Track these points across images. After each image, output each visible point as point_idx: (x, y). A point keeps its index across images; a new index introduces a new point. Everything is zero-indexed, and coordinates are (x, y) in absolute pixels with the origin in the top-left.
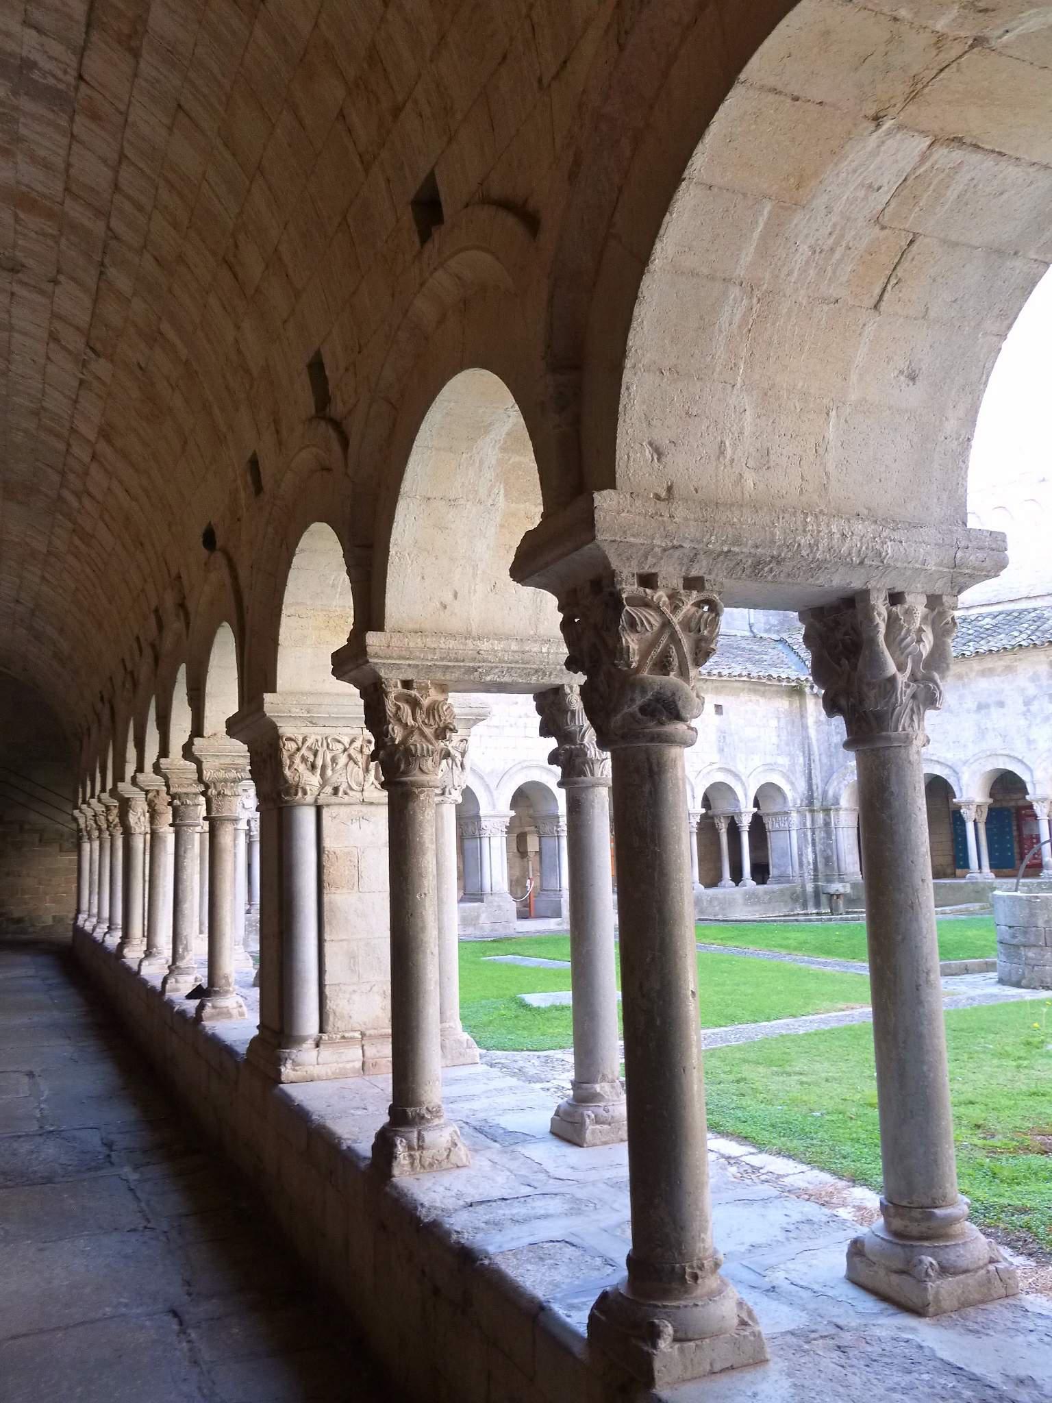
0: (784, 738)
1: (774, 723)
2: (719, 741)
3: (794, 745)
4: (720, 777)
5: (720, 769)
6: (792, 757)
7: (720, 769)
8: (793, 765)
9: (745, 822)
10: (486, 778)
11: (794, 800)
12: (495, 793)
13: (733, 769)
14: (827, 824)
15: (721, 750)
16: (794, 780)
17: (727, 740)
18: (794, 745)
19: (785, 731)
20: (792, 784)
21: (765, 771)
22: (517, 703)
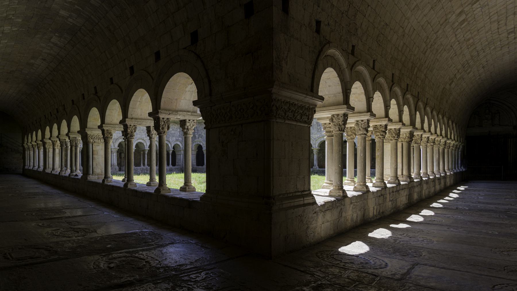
0: (181, 133)
6: (182, 138)
8: (182, 140)
9: (171, 152)
11: (182, 148)
13: (169, 140)
21: (176, 141)
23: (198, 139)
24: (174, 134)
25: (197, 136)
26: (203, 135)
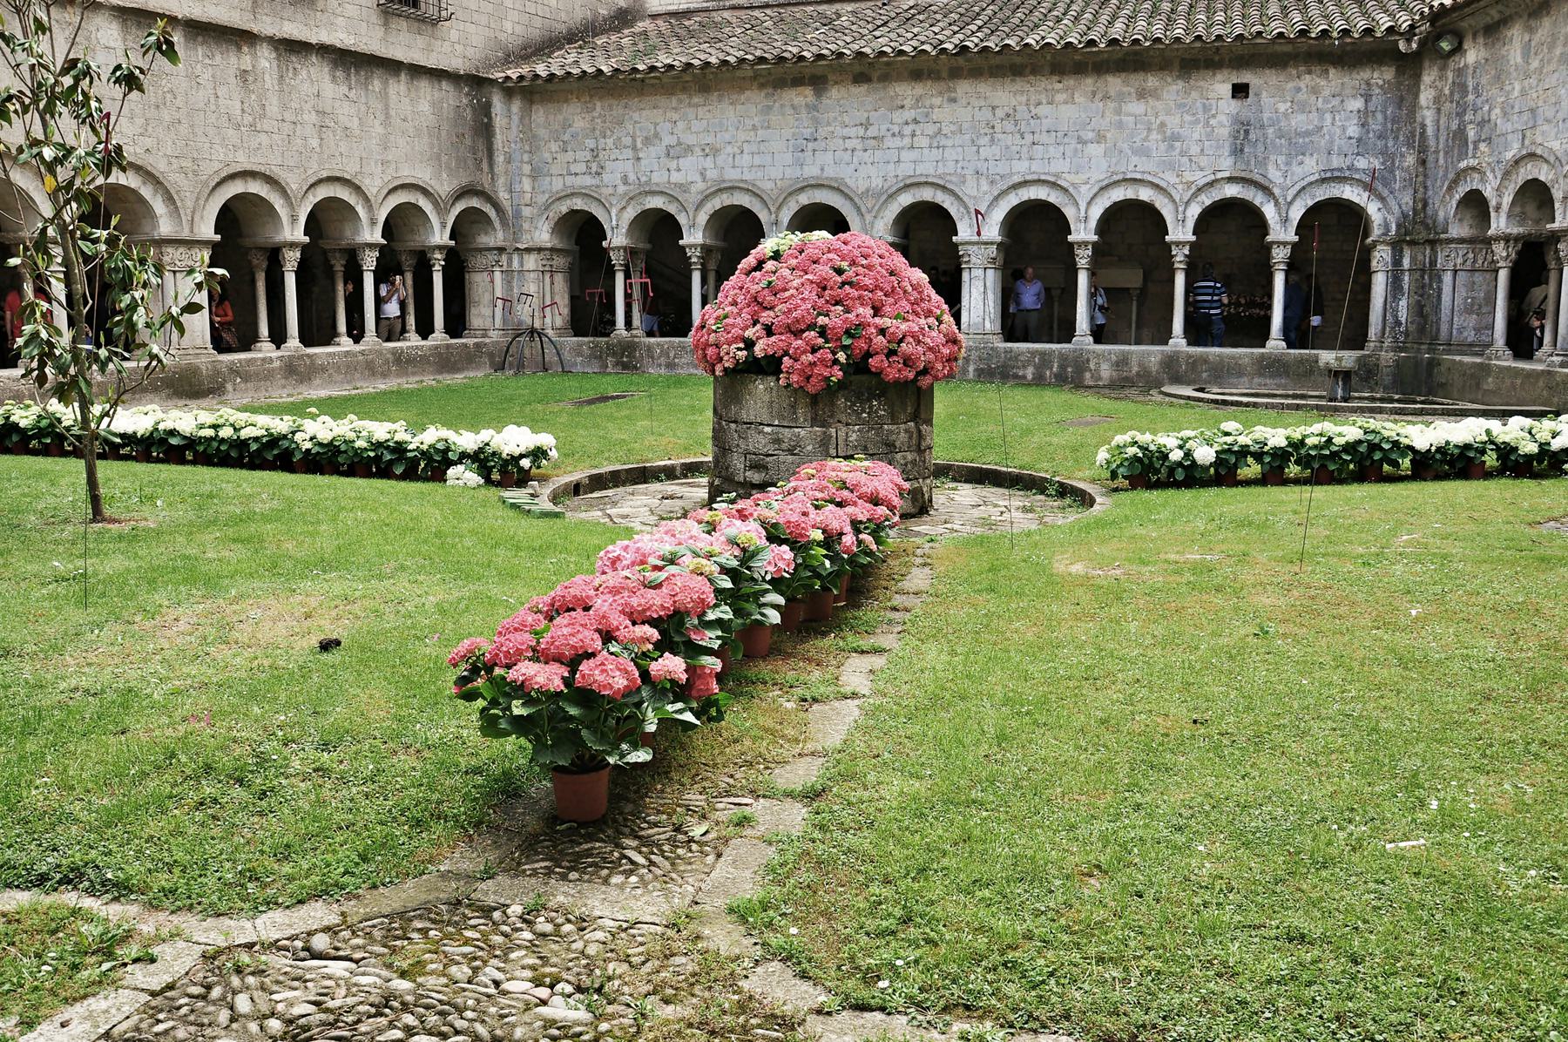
1: (1358, 104)
2: (1236, 138)
3: (1396, 138)
4: (1232, 191)
5: (1231, 179)
7: (1231, 179)
10: (856, 199)
11: (1387, 226)
12: (868, 218)
14: (1433, 262)
15: (1237, 151)
16: (1385, 193)
17: (1252, 136)
18: (1396, 138)
19: (1379, 116)
20: (1382, 199)
22: (902, 107)
23: (1474, 157)
24: (1307, 133)
25: (1471, 134)
26: (1498, 122)
